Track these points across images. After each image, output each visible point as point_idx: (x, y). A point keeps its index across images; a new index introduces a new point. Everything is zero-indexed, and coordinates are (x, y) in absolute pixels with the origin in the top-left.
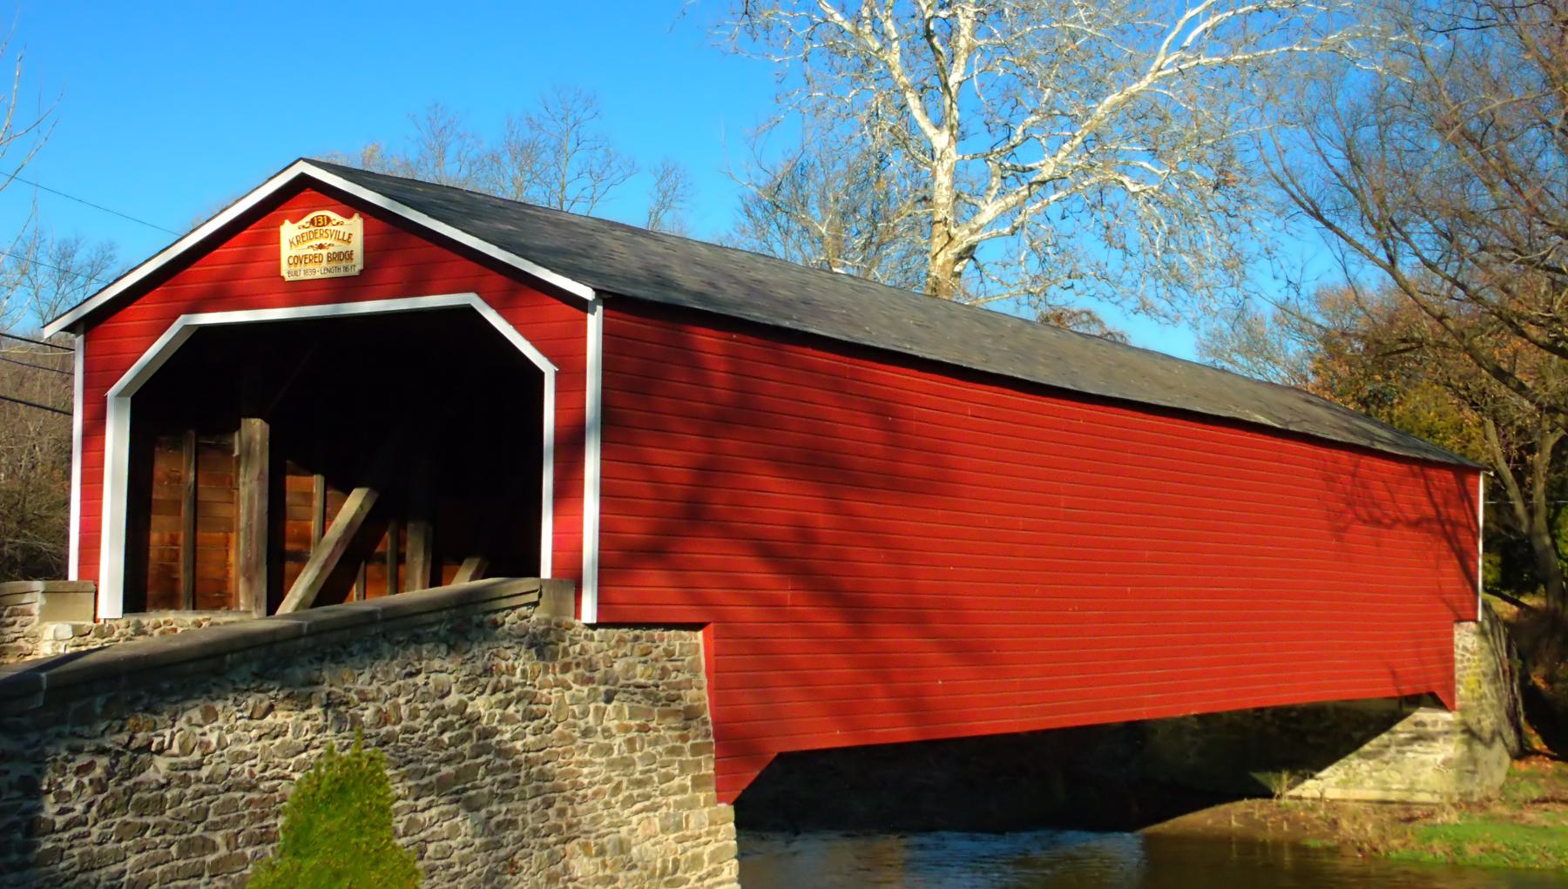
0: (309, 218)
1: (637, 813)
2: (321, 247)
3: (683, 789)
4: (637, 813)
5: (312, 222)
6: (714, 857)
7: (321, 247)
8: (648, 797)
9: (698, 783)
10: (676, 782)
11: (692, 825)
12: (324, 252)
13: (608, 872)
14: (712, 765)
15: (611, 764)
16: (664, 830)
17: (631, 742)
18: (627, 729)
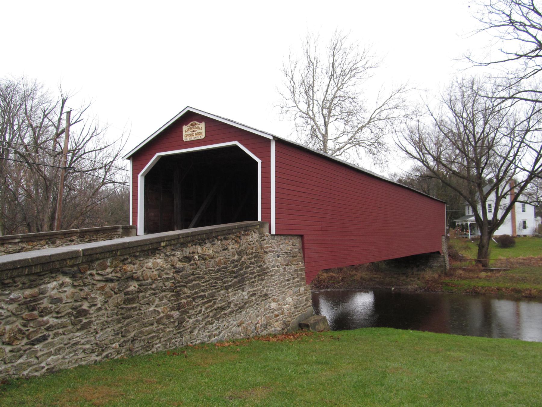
0: (190, 124)
1: (287, 289)
2: (194, 131)
3: (298, 282)
4: (287, 289)
5: (191, 125)
6: (306, 300)
7: (194, 131)
8: (289, 284)
9: (302, 279)
10: (296, 279)
11: (301, 291)
12: (194, 133)
13: (280, 306)
14: (305, 274)
15: (281, 275)
16: (294, 293)
17: (285, 269)
18: (282, 265)
